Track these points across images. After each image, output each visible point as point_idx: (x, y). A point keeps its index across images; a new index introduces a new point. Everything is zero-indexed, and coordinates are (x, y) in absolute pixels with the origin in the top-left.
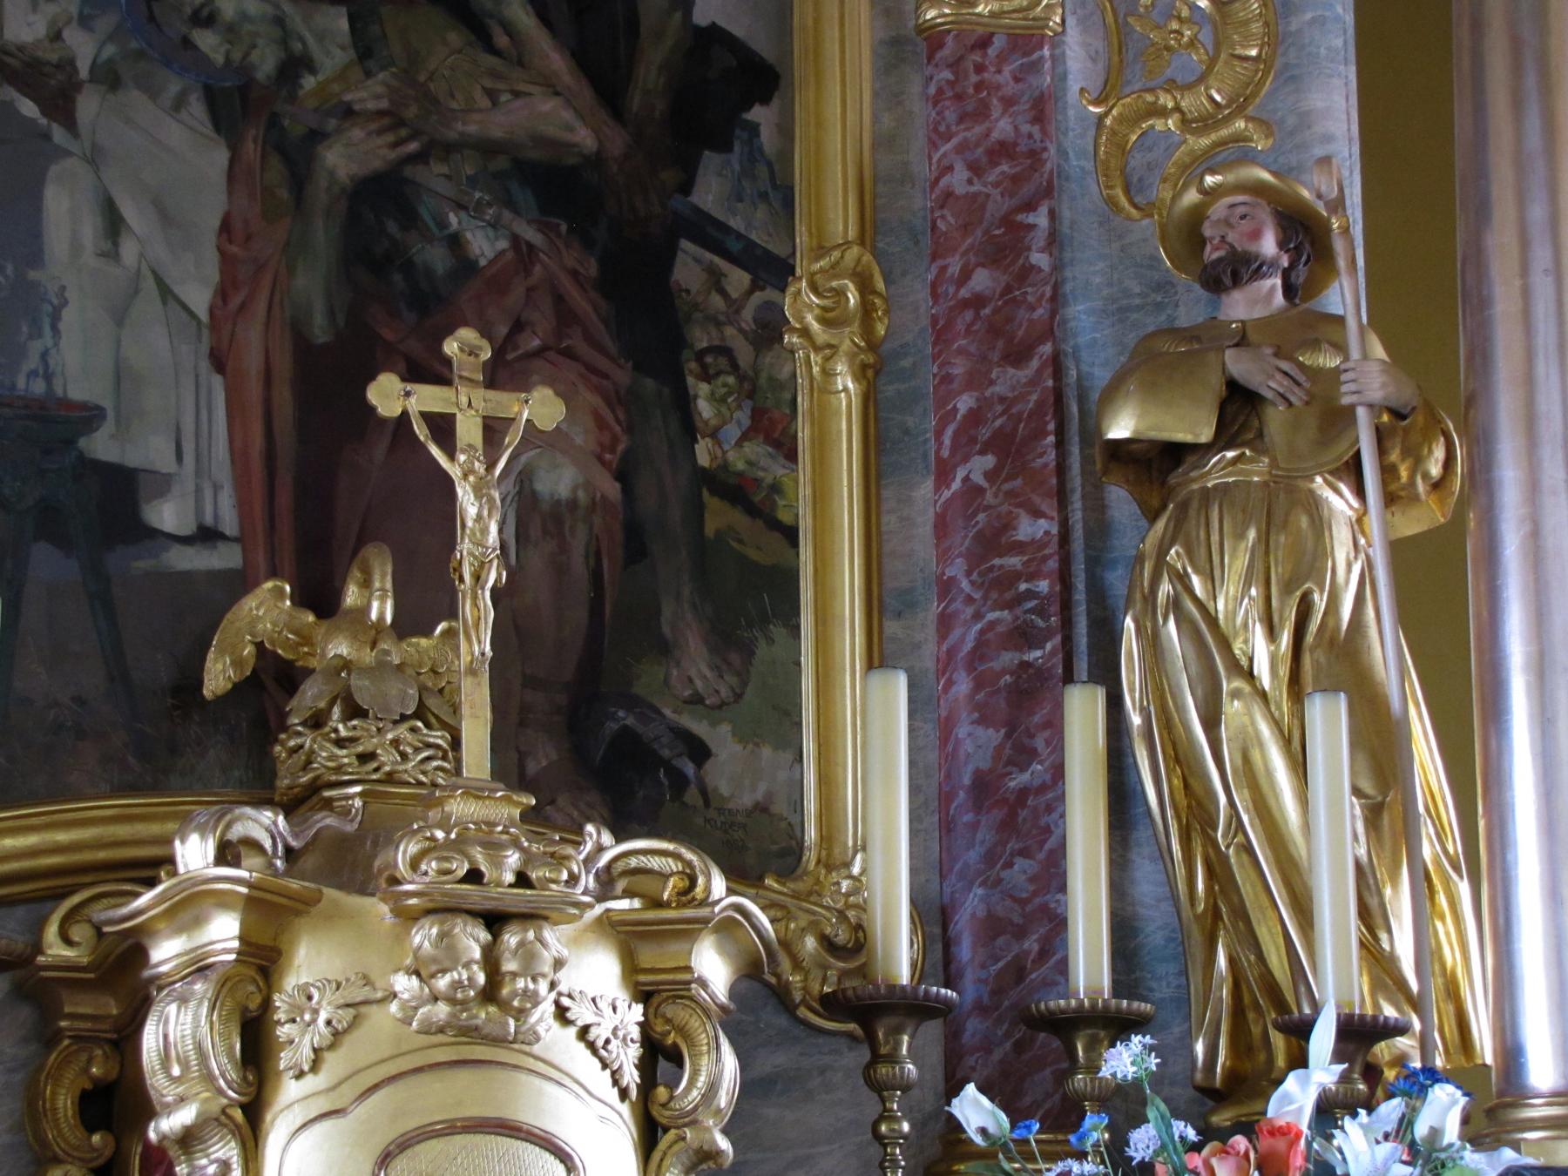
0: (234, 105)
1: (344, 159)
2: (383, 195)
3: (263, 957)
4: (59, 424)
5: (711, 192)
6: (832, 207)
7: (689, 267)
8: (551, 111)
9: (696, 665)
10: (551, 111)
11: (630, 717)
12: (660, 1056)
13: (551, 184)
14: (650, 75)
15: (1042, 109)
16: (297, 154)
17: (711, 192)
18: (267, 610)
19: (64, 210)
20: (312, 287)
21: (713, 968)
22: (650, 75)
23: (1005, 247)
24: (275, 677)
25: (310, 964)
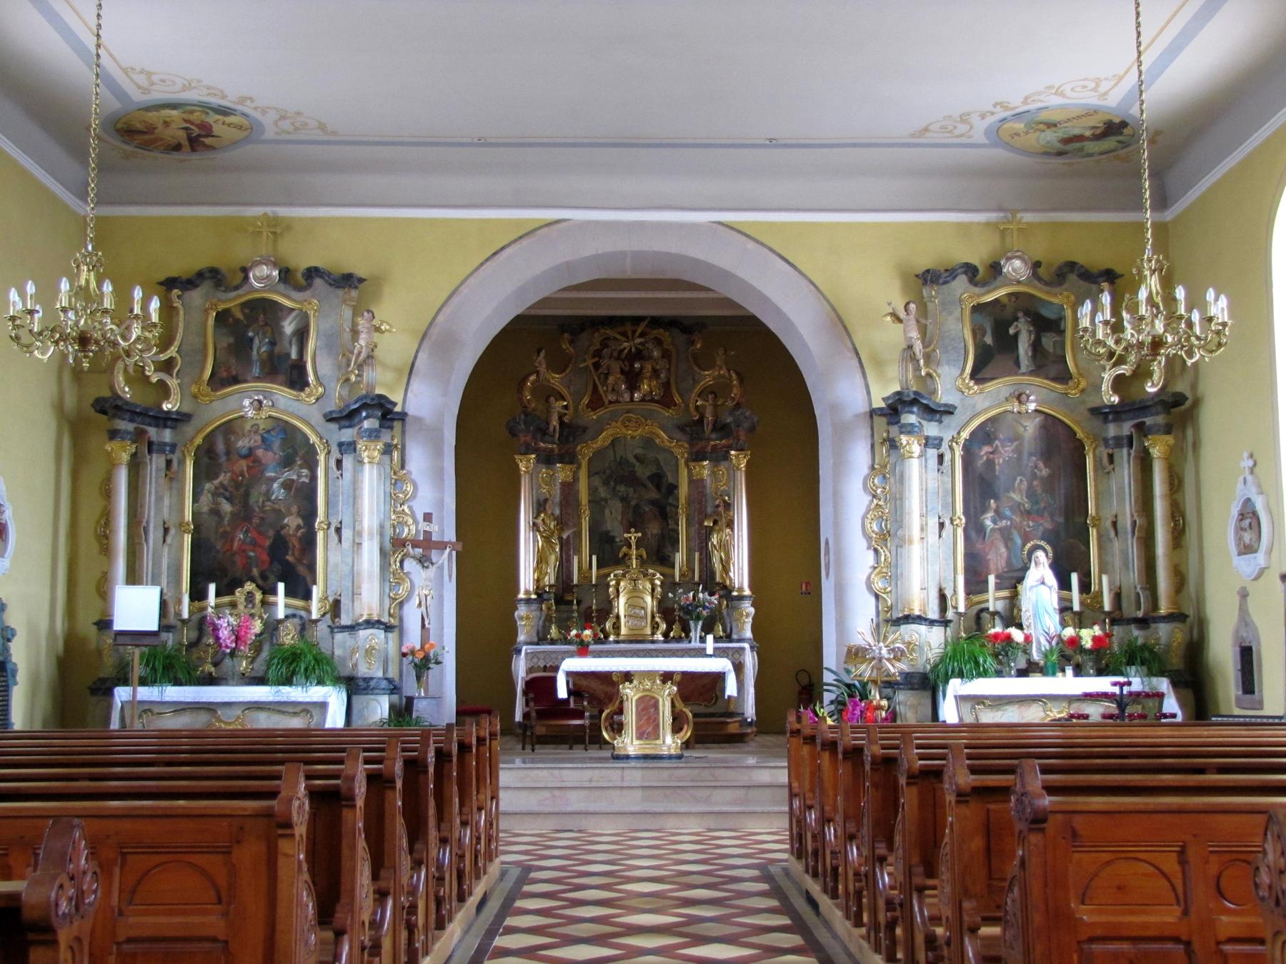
0: (624, 500)
1: (633, 503)
2: (637, 507)
3: (618, 584)
4: (607, 533)
5: (670, 500)
6: (682, 500)
7: (668, 509)
8: (654, 495)
9: (669, 548)
10: (654, 495)
11: (660, 556)
12: (653, 590)
13: (653, 502)
14: (664, 490)
15: (704, 487)
16: (628, 503)
17: (670, 500)
18: (625, 549)
19: (607, 512)
20: (630, 515)
21: (658, 582)
22: (664, 490)
23: (700, 503)
24: (625, 555)
25: (622, 584)
